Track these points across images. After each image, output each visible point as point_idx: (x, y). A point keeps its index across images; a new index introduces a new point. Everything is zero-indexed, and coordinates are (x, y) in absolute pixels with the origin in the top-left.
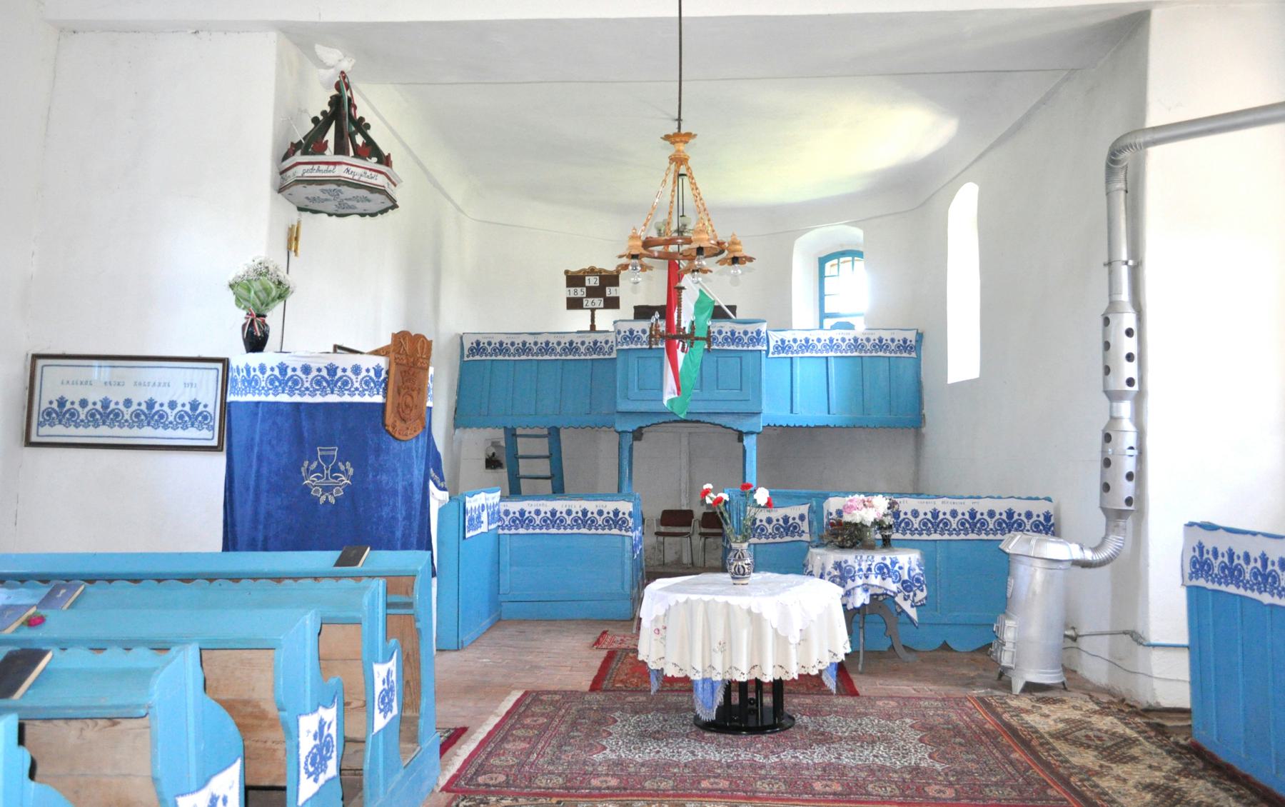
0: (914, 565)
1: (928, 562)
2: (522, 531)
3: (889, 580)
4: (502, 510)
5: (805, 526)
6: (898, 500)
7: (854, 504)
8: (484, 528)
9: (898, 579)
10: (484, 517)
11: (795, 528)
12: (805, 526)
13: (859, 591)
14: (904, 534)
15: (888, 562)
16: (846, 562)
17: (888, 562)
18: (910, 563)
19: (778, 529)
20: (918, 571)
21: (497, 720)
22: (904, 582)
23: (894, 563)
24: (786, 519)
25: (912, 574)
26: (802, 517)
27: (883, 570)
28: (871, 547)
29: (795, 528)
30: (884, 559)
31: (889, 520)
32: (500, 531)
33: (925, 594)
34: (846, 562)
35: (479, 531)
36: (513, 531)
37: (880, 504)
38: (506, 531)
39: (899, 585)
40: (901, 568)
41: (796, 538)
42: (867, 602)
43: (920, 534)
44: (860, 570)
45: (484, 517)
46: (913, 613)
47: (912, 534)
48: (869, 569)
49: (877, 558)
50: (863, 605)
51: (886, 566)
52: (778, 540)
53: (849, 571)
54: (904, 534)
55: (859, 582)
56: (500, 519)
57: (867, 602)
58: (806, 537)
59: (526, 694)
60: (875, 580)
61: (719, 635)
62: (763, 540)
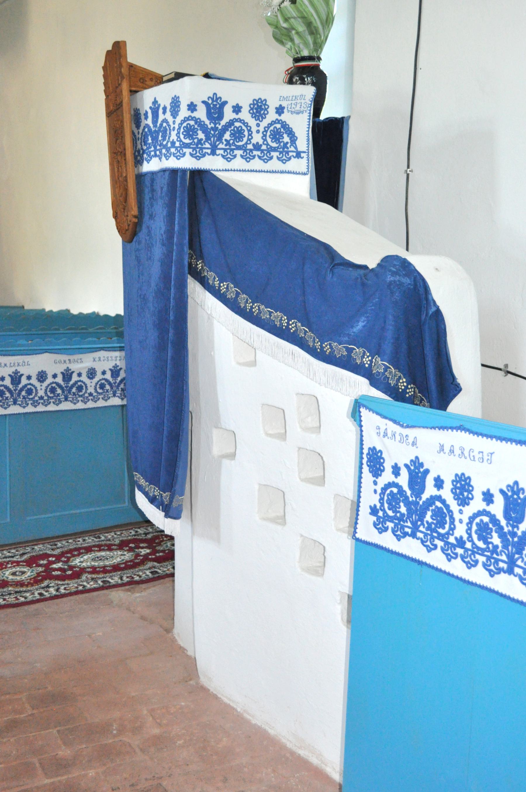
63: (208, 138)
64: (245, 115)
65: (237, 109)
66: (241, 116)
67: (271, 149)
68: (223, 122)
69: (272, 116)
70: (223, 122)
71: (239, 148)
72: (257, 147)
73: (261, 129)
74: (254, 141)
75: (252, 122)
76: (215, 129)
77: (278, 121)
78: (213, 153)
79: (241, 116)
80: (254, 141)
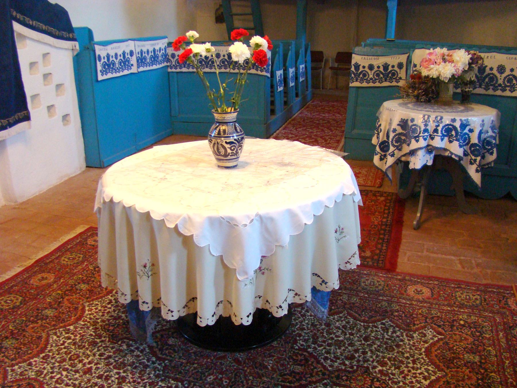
0: (487, 127)
1: (503, 128)
2: (184, 70)
3: (456, 144)
4: (170, 54)
5: (402, 74)
6: (482, 55)
7: (433, 57)
8: (134, 70)
9: (466, 141)
10: (133, 60)
11: (393, 74)
12: (402, 74)
13: (421, 153)
14: (487, 89)
15: (457, 125)
16: (412, 120)
17: (457, 125)
18: (483, 125)
19: (378, 75)
20: (490, 133)
21: (20, 269)
22: (474, 145)
23: (463, 126)
24: (386, 66)
25: (483, 136)
26: (400, 66)
27: (449, 131)
28: (447, 104)
29: (393, 74)
30: (454, 120)
31: (472, 76)
32: (170, 70)
33: (494, 156)
34: (412, 120)
35: (126, 72)
36: (178, 70)
37: (461, 57)
38: (174, 70)
39: (467, 148)
40: (471, 131)
41: (394, 84)
42: (430, 163)
43: (504, 90)
44: (426, 131)
45: (133, 60)
46: (476, 177)
47: (495, 90)
48: (436, 131)
49: (448, 117)
50: (425, 167)
51: (455, 128)
52: (377, 84)
53: (414, 131)
54: (487, 89)
55: (422, 143)
56: (168, 60)
57: (430, 163)
58: (401, 83)
59: (91, 228)
60: (438, 143)
61: (143, 256)
62: (365, 84)
63: (355, 76)
64: (367, 69)
65: (364, 67)
66: (365, 69)
67: (376, 79)
68: (359, 71)
69: (376, 69)
70: (359, 71)
71: (365, 80)
72: (371, 79)
73: (372, 73)
74: (370, 77)
75: (369, 71)
76: (357, 73)
77: (377, 71)
78: (357, 81)
79: (365, 69)
80: (370, 77)
